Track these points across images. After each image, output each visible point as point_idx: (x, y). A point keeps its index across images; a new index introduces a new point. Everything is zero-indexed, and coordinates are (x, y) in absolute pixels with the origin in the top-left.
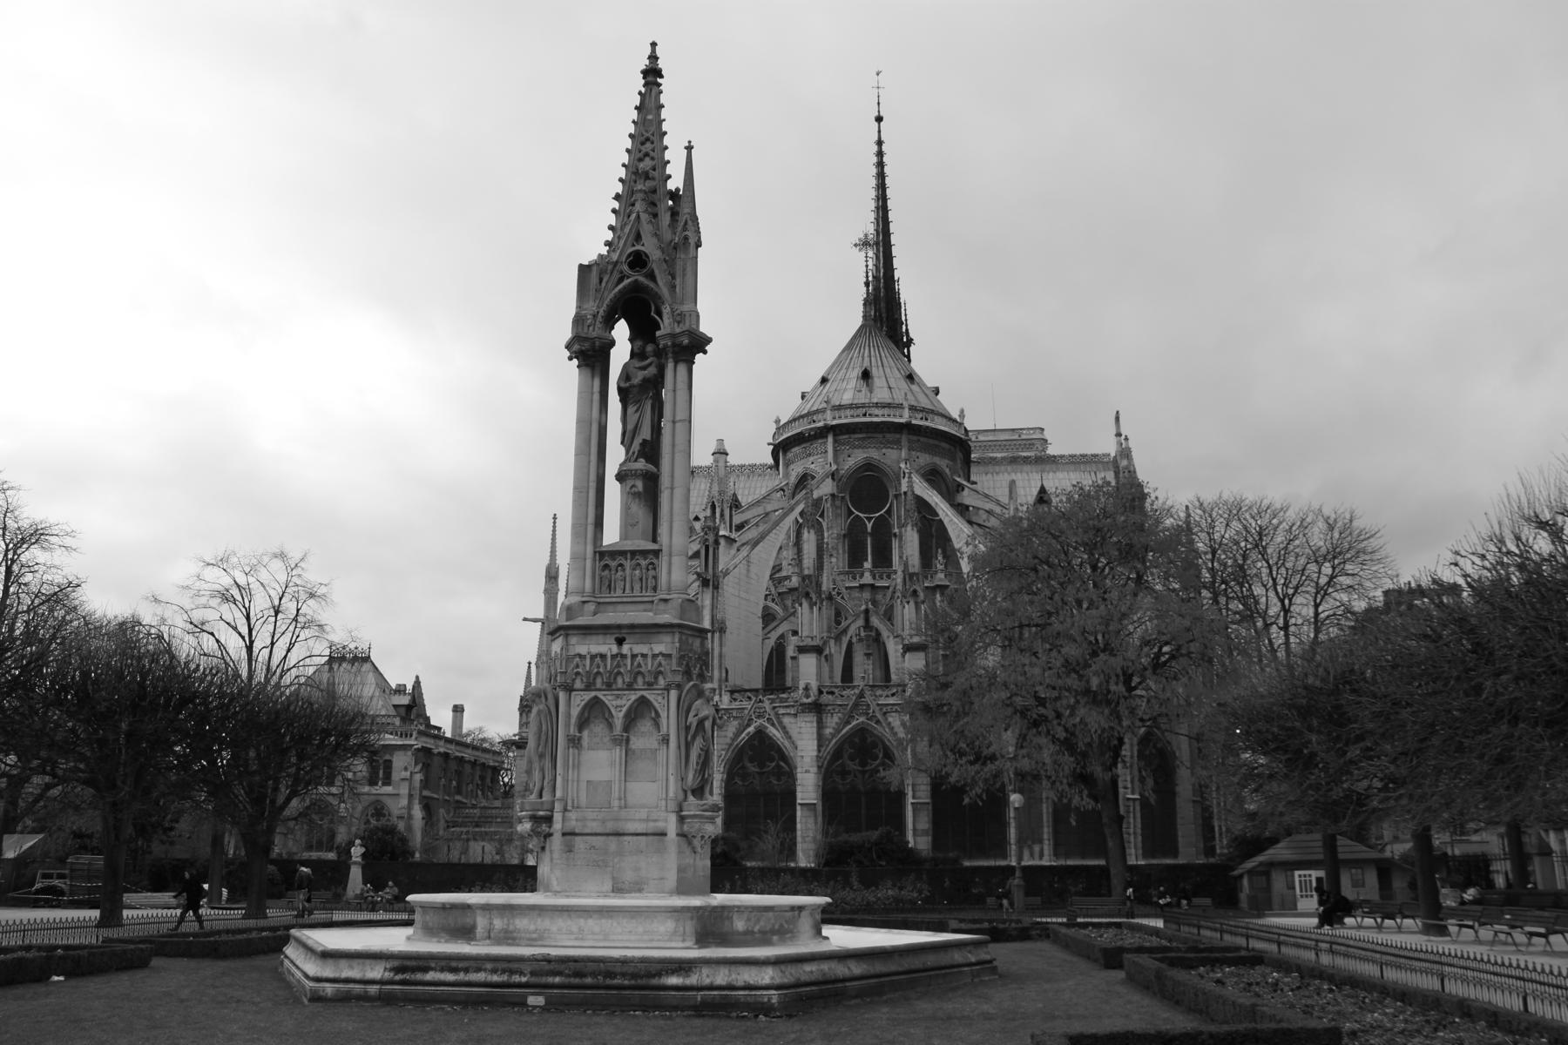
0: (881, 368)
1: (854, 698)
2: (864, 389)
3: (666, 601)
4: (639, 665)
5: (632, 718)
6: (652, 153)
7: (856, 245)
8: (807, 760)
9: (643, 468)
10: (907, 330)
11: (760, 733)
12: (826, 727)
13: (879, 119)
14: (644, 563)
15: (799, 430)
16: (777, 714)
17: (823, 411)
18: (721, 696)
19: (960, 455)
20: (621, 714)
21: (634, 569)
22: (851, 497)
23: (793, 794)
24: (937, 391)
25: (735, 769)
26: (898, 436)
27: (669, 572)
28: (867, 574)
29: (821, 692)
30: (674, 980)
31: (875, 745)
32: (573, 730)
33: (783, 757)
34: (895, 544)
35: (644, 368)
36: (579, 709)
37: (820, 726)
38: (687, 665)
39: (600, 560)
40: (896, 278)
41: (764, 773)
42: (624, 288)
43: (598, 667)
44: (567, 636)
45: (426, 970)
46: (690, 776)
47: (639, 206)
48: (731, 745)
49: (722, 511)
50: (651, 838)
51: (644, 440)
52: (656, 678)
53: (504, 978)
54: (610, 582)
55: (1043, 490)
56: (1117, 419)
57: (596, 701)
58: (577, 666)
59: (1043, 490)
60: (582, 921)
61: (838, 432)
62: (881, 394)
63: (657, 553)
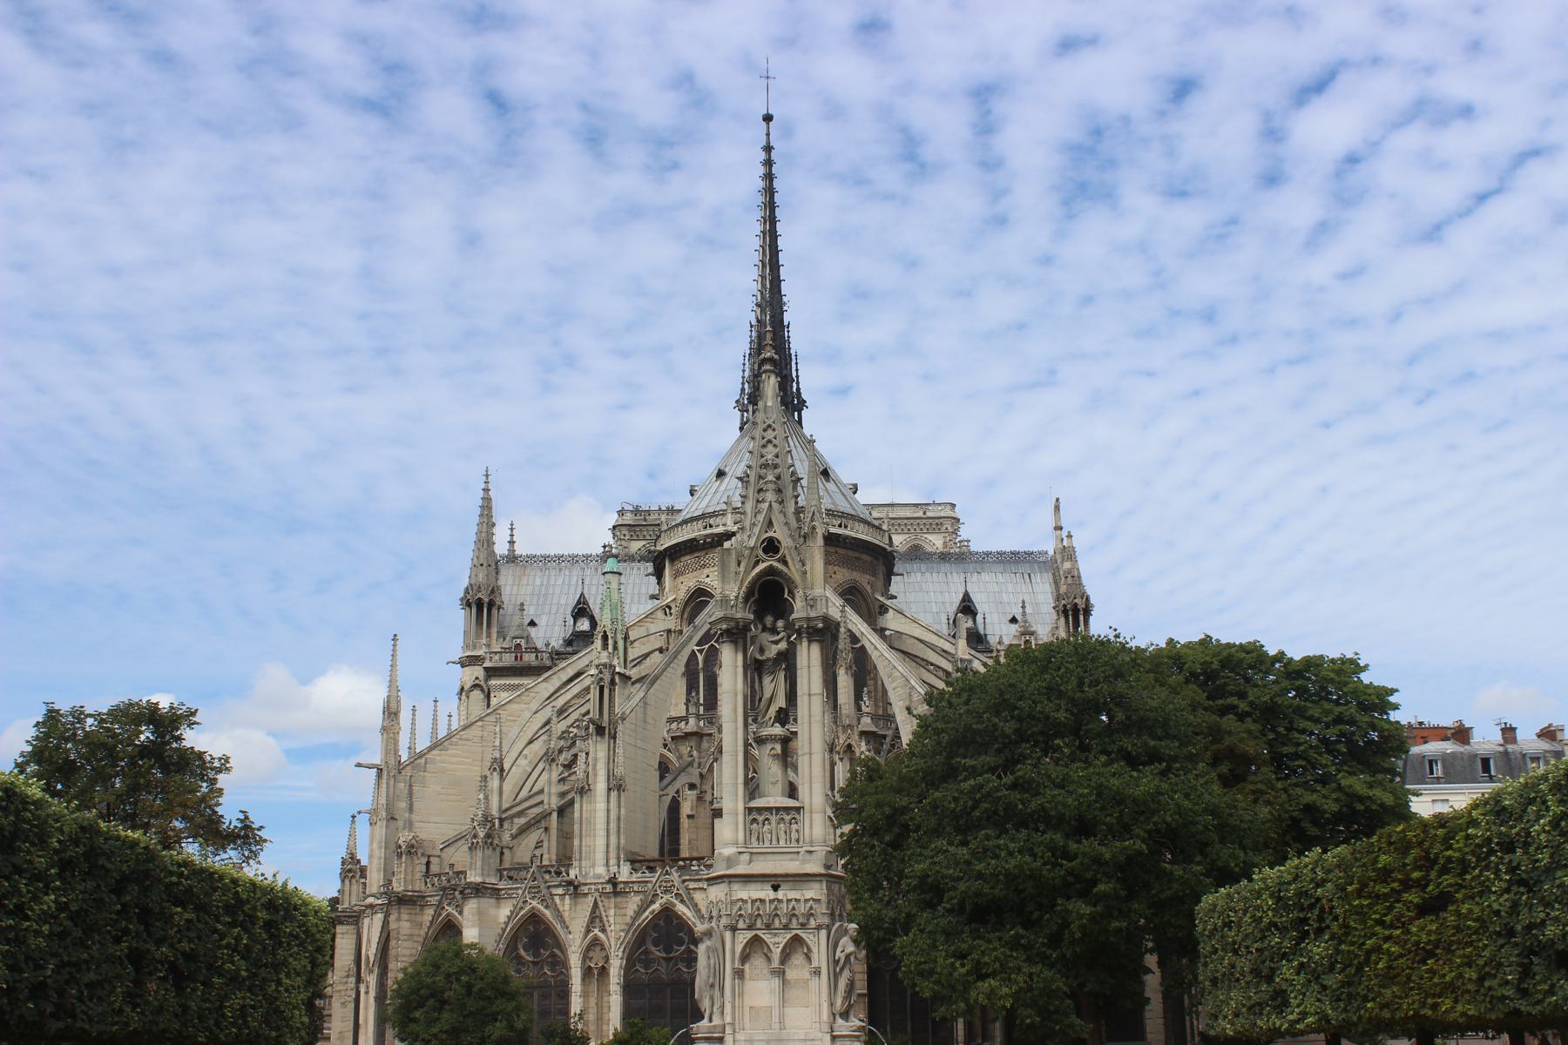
3: (811, 852)
5: (786, 956)
10: (798, 389)
11: (667, 913)
13: (768, 118)
14: (787, 818)
15: (692, 536)
17: (723, 513)
18: (619, 867)
19: (881, 569)
20: (779, 950)
21: (779, 823)
24: (855, 489)
27: (811, 828)
35: (776, 643)
36: (742, 945)
39: (749, 814)
40: (786, 323)
41: (672, 958)
43: (758, 909)
46: (839, 1002)
47: (770, 496)
48: (632, 924)
49: (616, 643)
52: (808, 920)
55: (966, 598)
56: (1057, 508)
57: (756, 939)
59: (966, 598)
63: (798, 810)
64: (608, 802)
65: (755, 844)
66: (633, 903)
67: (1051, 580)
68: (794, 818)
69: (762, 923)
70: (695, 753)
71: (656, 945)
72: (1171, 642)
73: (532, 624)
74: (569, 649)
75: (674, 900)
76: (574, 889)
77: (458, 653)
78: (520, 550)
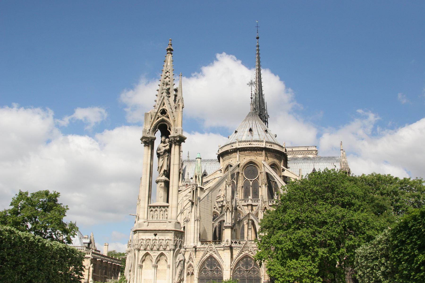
0: (256, 128)
1: (244, 245)
2: (250, 135)
3: (170, 222)
5: (158, 261)
6: (169, 76)
7: (248, 84)
9: (164, 179)
10: (267, 112)
11: (211, 257)
14: (164, 209)
20: (155, 258)
22: (245, 173)
25: (202, 269)
28: (250, 201)
29: (232, 242)
32: (140, 263)
33: (219, 265)
38: (176, 243)
39: (150, 208)
40: (263, 94)
41: (212, 271)
42: (159, 121)
43: (148, 243)
47: (165, 94)
51: (165, 170)
54: (153, 215)
57: (147, 254)
58: (142, 242)
62: (256, 137)
63: (168, 207)
65: (151, 219)
67: (340, 165)
68: (166, 210)
71: (208, 266)
72: (363, 175)
75: (213, 253)
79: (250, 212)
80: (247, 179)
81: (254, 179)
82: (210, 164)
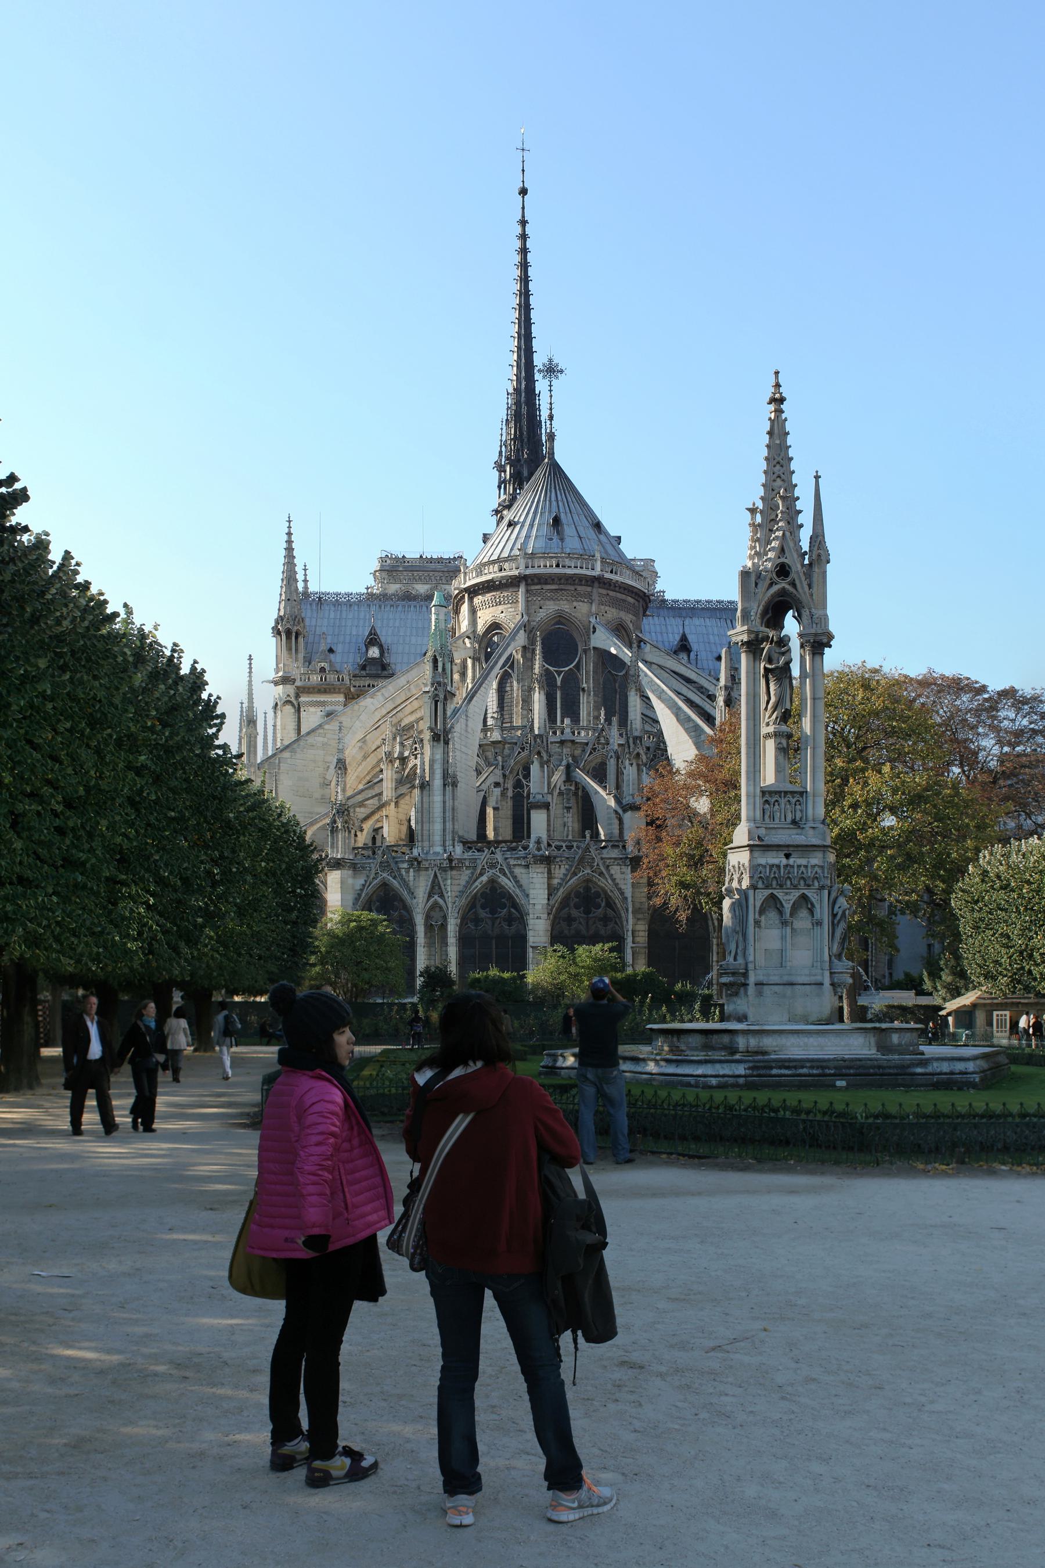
4: (802, 873)
8: (538, 907)
12: (555, 878)
16: (508, 865)
18: (454, 847)
23: (522, 938)
25: (469, 917)
26: (589, 589)
30: (919, 1070)
31: (597, 895)
32: (757, 916)
33: (515, 905)
34: (583, 699)
37: (550, 877)
41: (497, 918)
43: (775, 873)
44: (751, 851)
45: (771, 1068)
49: (444, 664)
50: (813, 986)
52: (813, 881)
53: (819, 1071)
55: (684, 638)
57: (772, 896)
58: (760, 873)
59: (684, 638)
60: (806, 1040)
61: (529, 581)
63: (801, 794)
64: (444, 795)
66: (465, 875)
69: (777, 884)
70: (500, 758)
73: (331, 651)
74: (363, 673)
75: (498, 874)
76: (416, 863)
77: (272, 675)
78: (313, 588)
79: (568, 761)
80: (547, 666)
81: (567, 669)
82: (380, 607)
